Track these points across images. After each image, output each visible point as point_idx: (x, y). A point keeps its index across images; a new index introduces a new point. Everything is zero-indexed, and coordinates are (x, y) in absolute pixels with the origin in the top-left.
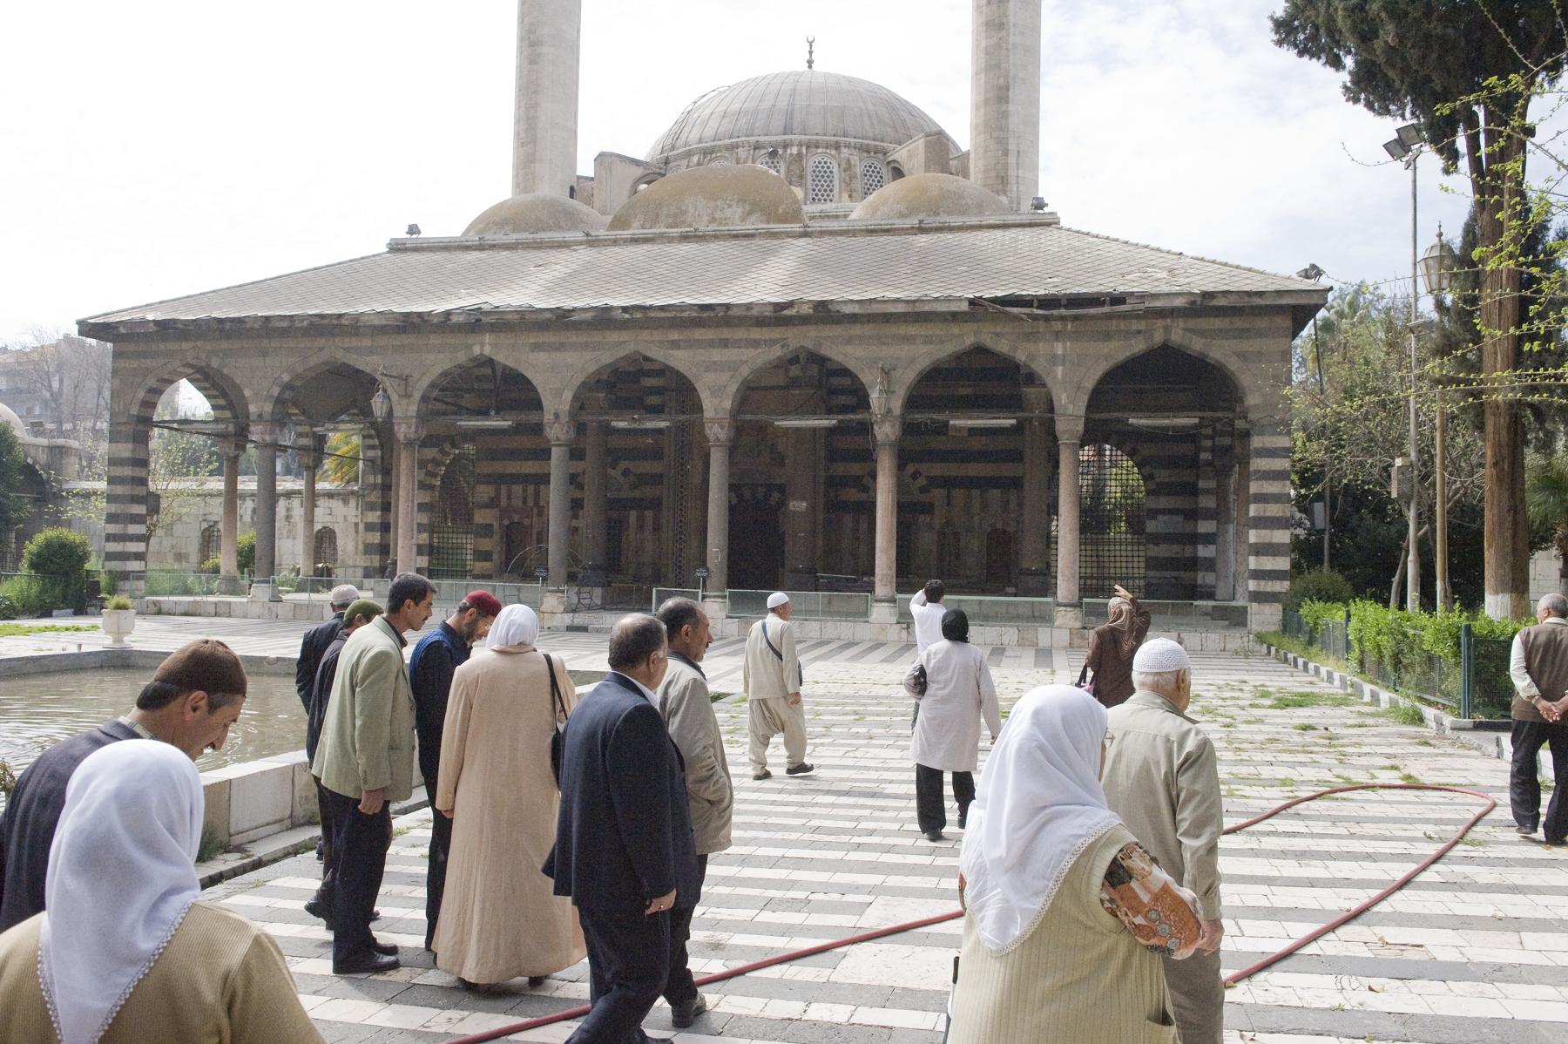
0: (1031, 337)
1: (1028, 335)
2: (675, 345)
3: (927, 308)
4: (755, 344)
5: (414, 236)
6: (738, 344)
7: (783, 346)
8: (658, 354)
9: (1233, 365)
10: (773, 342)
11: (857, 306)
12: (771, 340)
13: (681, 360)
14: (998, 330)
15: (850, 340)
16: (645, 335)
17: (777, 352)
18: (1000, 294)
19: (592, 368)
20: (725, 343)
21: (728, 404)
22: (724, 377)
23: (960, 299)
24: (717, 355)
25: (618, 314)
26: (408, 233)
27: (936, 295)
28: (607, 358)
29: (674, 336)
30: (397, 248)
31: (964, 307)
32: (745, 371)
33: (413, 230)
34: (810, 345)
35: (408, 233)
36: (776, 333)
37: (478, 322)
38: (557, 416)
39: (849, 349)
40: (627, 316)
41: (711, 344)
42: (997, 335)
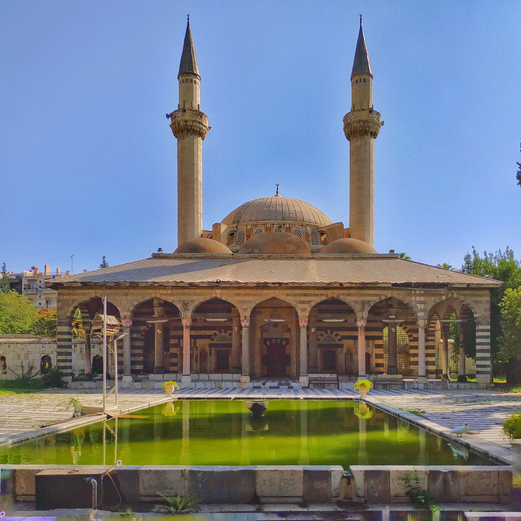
0: (410, 295)
1: (409, 294)
2: (288, 295)
3: (378, 285)
4: (317, 295)
5: (160, 252)
6: (310, 295)
7: (326, 296)
8: (282, 298)
9: (472, 305)
10: (322, 295)
11: (354, 284)
12: (322, 294)
13: (290, 300)
14: (399, 293)
15: (349, 295)
16: (277, 292)
17: (324, 298)
18: (402, 282)
19: (258, 302)
20: (306, 295)
21: (307, 314)
22: (306, 306)
23: (389, 283)
24: (304, 299)
25: (271, 285)
26: (158, 251)
27: (381, 282)
28: (263, 299)
29: (288, 292)
30: (155, 256)
31: (390, 286)
32: (313, 304)
33: (160, 250)
34: (335, 296)
35: (158, 251)
36: (324, 292)
37: (216, 285)
38: (245, 317)
39: (349, 298)
40: (273, 285)
41: (301, 295)
42: (398, 294)
